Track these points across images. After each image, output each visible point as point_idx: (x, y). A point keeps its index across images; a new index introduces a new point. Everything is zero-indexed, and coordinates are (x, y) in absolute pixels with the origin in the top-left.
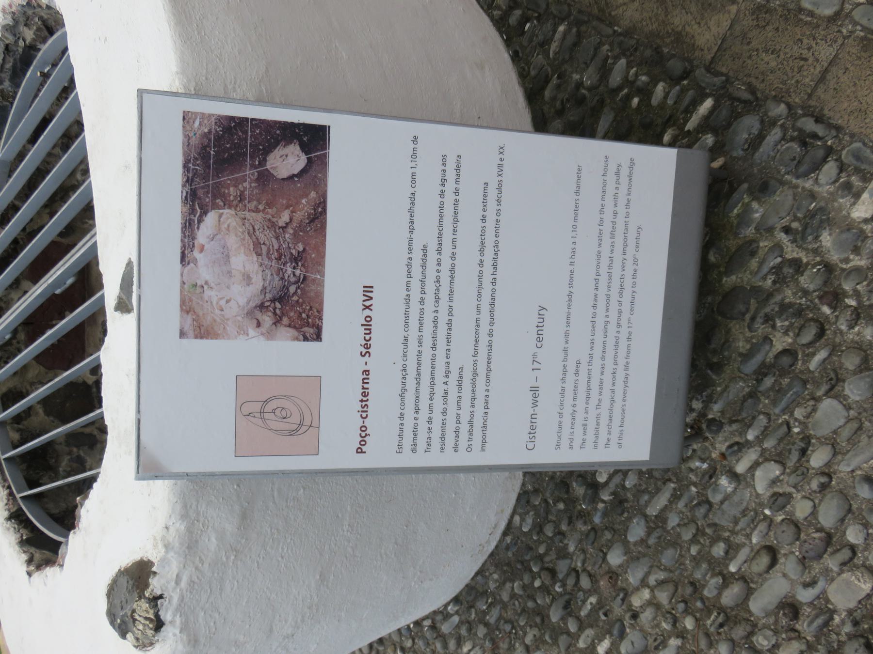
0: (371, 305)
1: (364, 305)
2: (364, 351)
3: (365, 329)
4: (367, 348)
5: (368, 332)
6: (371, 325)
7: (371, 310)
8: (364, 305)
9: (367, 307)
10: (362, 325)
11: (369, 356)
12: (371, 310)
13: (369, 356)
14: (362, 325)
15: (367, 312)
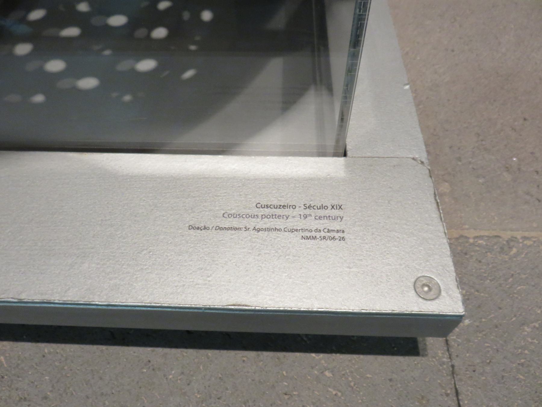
0: (334, 209)
1: (334, 205)
2: (307, 206)
3: (320, 206)
4: (309, 207)
5: (319, 208)
6: (322, 209)
7: (331, 209)
8: (334, 205)
9: (333, 207)
10: (322, 205)
11: (304, 209)
12: (331, 209)
13: (304, 209)
14: (322, 205)
15: (330, 207)
